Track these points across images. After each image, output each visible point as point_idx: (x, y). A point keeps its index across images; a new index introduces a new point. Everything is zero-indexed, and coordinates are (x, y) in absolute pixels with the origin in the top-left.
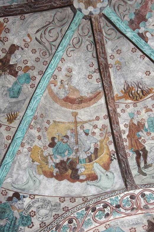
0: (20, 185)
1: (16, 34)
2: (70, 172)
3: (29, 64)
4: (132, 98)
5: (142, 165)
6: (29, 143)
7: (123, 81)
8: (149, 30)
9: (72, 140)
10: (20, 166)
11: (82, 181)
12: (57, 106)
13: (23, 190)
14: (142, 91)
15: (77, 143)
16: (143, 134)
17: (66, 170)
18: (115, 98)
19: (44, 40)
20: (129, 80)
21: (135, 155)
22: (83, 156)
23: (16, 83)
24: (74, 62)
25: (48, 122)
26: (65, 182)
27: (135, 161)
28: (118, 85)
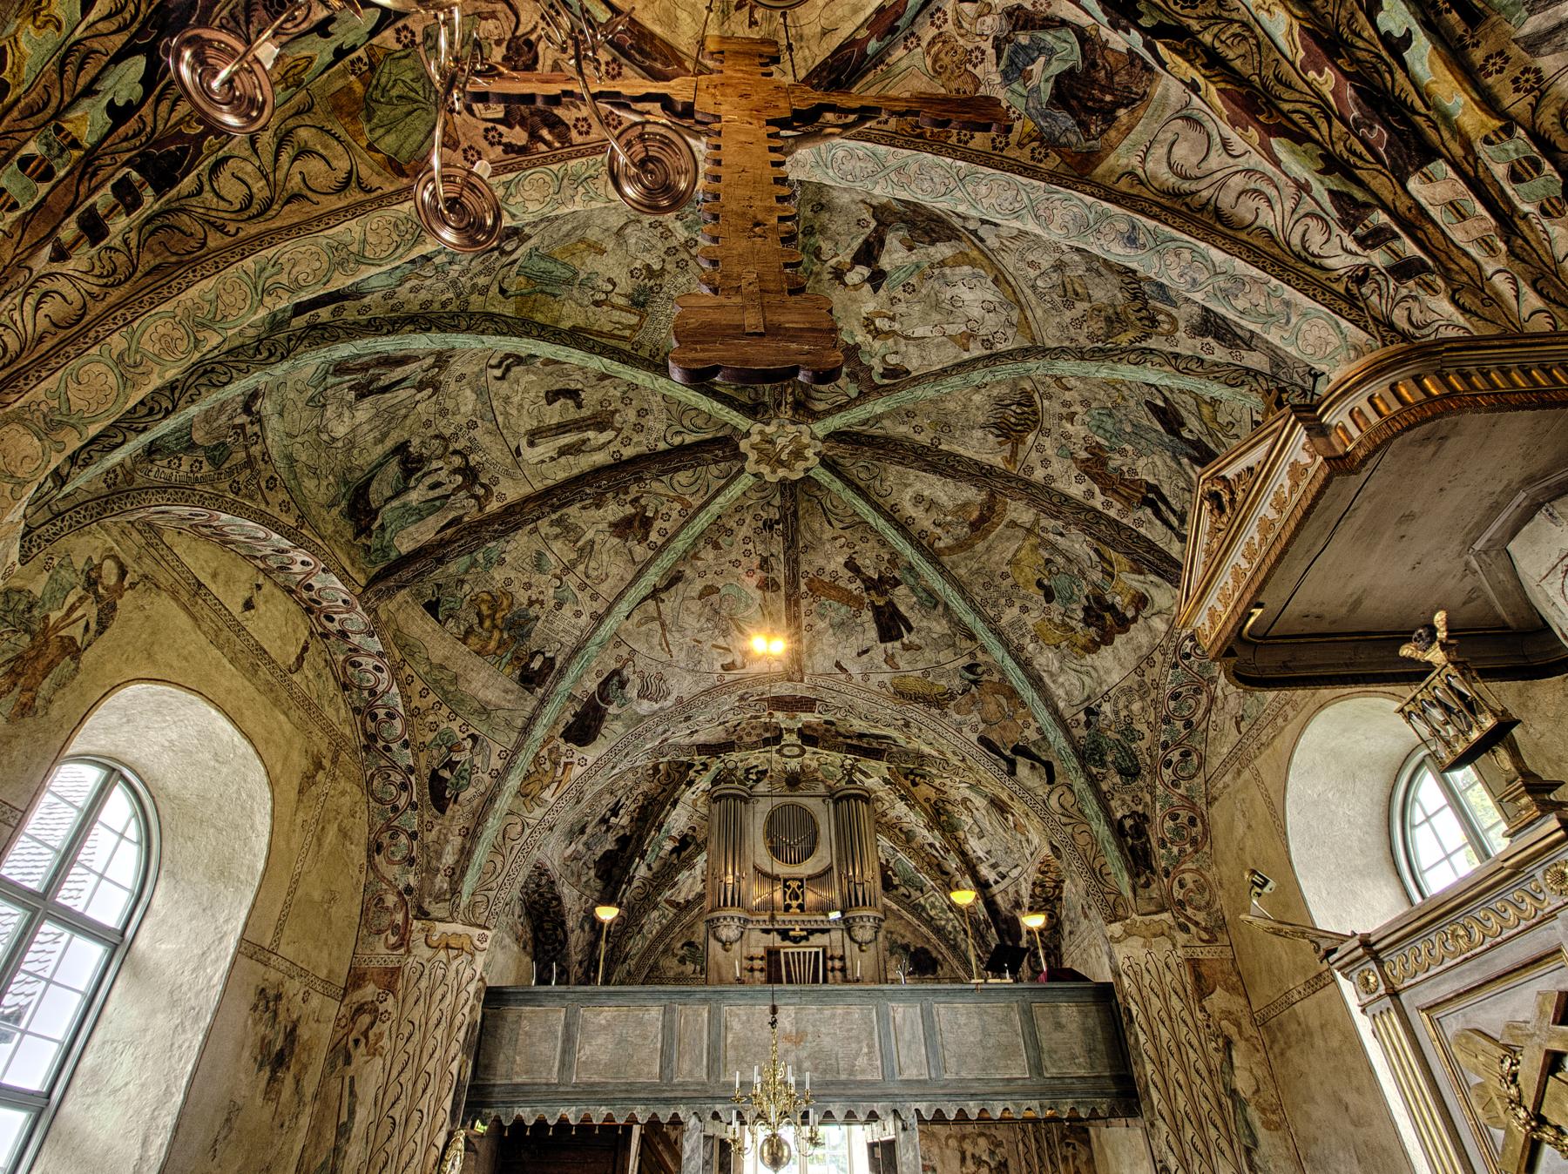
0: (1078, 696)
1: (828, 557)
2: (1108, 615)
3: (886, 557)
4: (1029, 429)
5: (1175, 522)
6: (1023, 635)
7: (978, 433)
8: (883, 351)
9: (1060, 560)
10: (1051, 674)
11: (1134, 619)
12: (980, 546)
13: (1089, 698)
14: (1019, 404)
15: (1069, 561)
16: (1116, 461)
17: (1103, 618)
18: (1010, 467)
19: (848, 520)
20: (981, 419)
21: (1149, 511)
22: (1096, 576)
23: (913, 589)
24: (906, 485)
25: (1004, 576)
26: (1119, 639)
27: (1158, 522)
28: (980, 447)
